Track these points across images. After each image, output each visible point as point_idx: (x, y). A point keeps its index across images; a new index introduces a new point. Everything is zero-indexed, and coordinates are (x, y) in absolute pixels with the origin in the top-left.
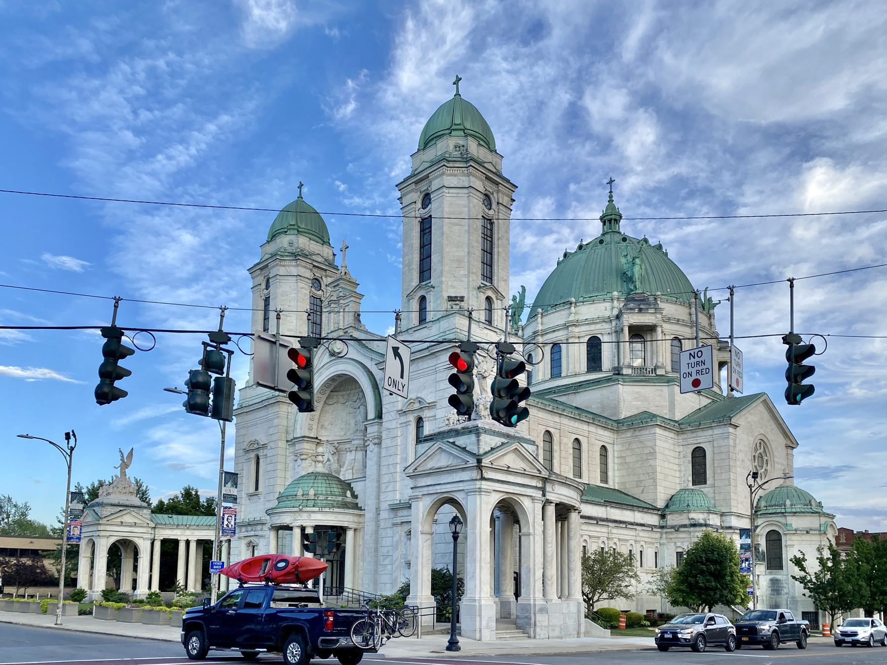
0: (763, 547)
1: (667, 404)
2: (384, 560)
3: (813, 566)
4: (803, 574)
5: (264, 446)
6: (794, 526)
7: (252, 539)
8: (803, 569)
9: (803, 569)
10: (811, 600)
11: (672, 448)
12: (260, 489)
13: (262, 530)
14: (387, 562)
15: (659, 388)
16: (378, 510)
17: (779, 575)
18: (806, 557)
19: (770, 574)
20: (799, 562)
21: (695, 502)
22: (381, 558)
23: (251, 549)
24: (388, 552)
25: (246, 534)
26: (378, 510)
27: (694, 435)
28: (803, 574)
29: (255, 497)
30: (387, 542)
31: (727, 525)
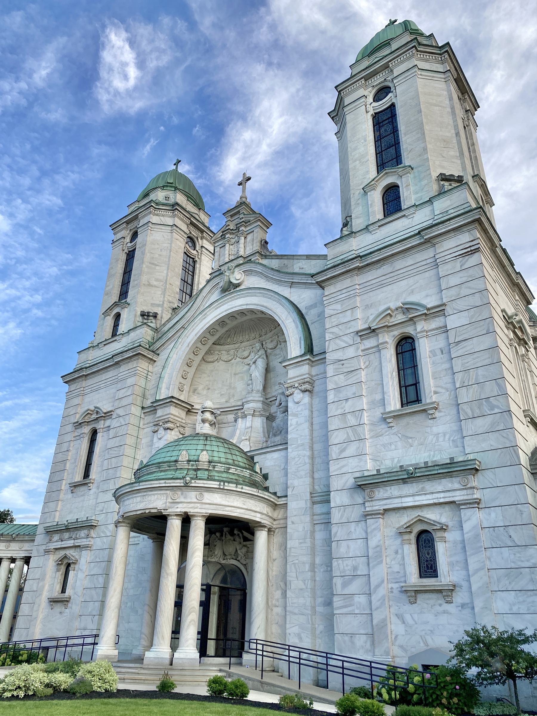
2: (345, 585)
5: (108, 415)
7: (69, 552)
12: (93, 475)
13: (88, 536)
14: (355, 587)
16: (322, 498)
22: (338, 582)
23: (63, 568)
24: (355, 568)
25: (59, 545)
26: (322, 498)
29: (82, 488)
30: (349, 548)
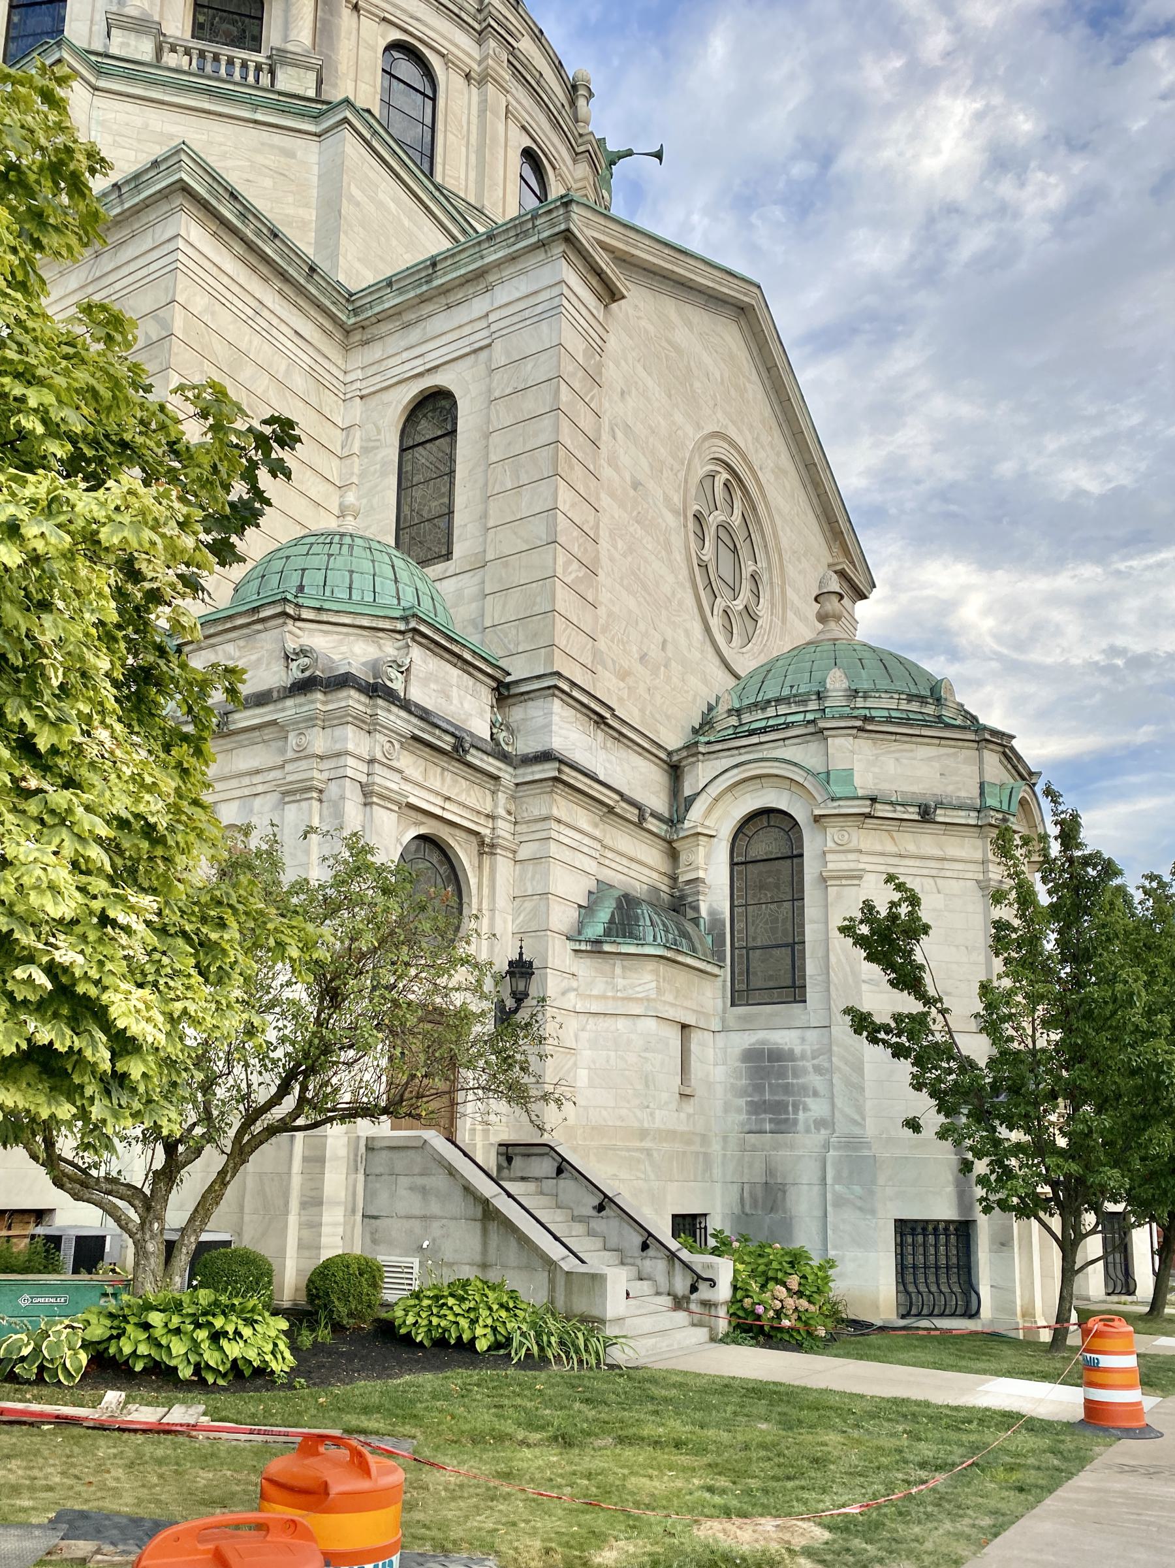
0: (715, 893)
1: (311, 215)
3: (959, 959)
4: (909, 1004)
6: (864, 782)
8: (908, 978)
9: (908, 978)
10: (945, 1154)
11: (299, 382)
15: (278, 139)
17: (783, 1030)
18: (925, 915)
19: (746, 1026)
20: (890, 941)
21: (339, 579)
27: (415, 335)
28: (909, 1004)
31: (525, 745)
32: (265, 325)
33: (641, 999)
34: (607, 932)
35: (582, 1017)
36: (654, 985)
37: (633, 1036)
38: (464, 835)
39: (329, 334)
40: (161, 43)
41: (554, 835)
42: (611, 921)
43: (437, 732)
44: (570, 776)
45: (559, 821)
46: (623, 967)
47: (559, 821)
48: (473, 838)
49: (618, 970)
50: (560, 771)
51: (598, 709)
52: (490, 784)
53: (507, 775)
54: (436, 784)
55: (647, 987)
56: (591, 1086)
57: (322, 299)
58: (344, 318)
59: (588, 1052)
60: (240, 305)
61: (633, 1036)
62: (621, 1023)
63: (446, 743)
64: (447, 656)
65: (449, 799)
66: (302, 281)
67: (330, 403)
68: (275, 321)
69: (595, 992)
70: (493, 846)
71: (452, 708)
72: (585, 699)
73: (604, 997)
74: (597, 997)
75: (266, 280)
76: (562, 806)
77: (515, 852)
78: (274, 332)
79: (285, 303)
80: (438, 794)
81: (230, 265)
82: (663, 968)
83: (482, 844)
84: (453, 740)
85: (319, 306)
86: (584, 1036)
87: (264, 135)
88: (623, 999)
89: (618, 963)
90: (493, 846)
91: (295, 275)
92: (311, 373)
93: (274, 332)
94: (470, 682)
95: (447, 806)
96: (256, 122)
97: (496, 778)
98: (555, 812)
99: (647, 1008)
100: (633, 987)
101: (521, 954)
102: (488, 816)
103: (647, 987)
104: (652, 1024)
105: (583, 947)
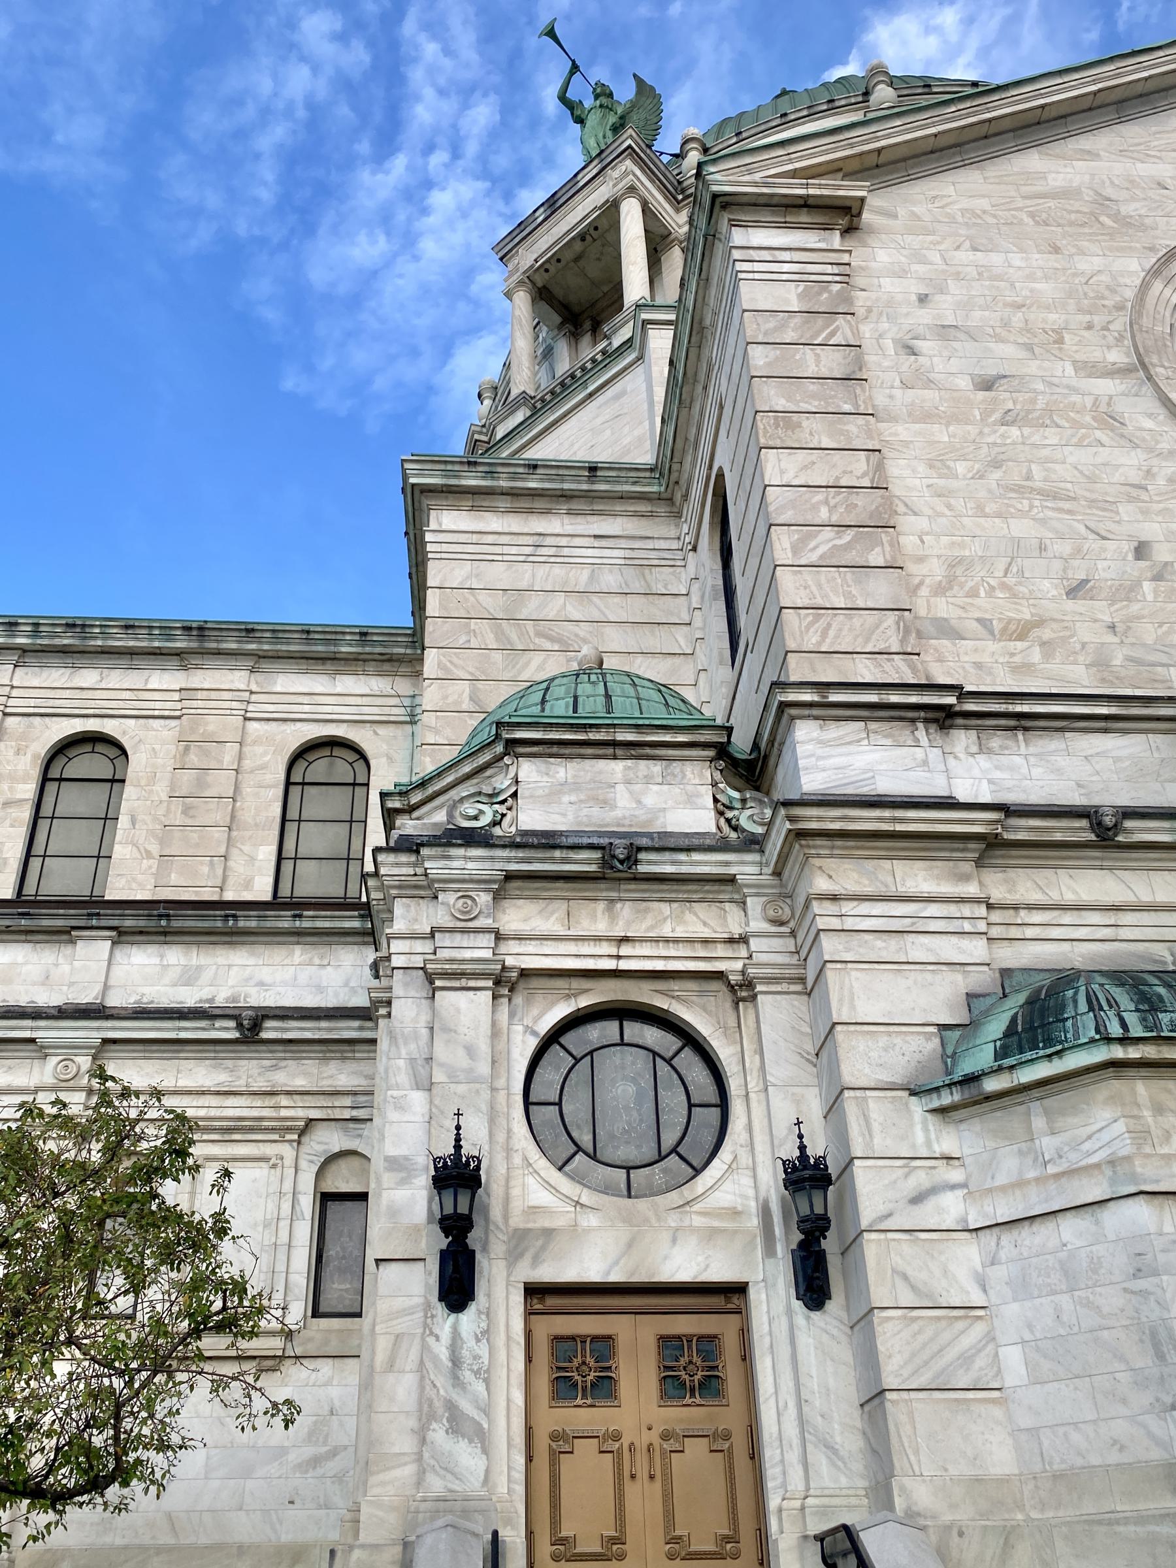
15: (610, 392)
32: (552, 551)
33: (1097, 1166)
34: (1001, 1053)
35: (989, 1238)
36: (1120, 1127)
37: (1099, 1250)
38: (691, 985)
39: (651, 515)
40: (533, 405)
41: (821, 923)
42: (1010, 1032)
43: (557, 854)
44: (814, 819)
45: (834, 898)
46: (1047, 1113)
47: (834, 898)
48: (715, 985)
49: (1039, 1123)
50: (791, 819)
51: (913, 699)
52: (726, 893)
53: (745, 867)
54: (601, 927)
55: (1106, 1136)
56: (1036, 1380)
57: (618, 488)
58: (655, 489)
59: (1015, 1307)
60: (514, 550)
61: (1099, 1250)
62: (1070, 1229)
63: (585, 861)
64: (589, 751)
65: (624, 940)
66: (585, 487)
67: (662, 579)
68: (564, 541)
69: (1001, 1180)
70: (749, 984)
71: (618, 813)
72: (872, 698)
73: (1020, 1184)
74: (1003, 1189)
75: (548, 512)
76: (831, 874)
77: (802, 980)
78: (566, 551)
79: (580, 519)
80: (598, 939)
81: (514, 523)
82: (1142, 1088)
83: (732, 988)
84: (597, 855)
85: (622, 497)
86: (998, 1274)
87: (600, 399)
88: (1057, 1176)
89: (1036, 1106)
90: (749, 984)
91: (573, 486)
92: (629, 563)
93: (566, 551)
94: (656, 768)
95: (625, 950)
96: (591, 395)
97: (731, 880)
98: (822, 884)
99: (1113, 1182)
100: (1076, 1145)
101: (802, 1148)
102: (731, 941)
103: (1106, 1136)
104: (1140, 1213)
105: (946, 1099)
